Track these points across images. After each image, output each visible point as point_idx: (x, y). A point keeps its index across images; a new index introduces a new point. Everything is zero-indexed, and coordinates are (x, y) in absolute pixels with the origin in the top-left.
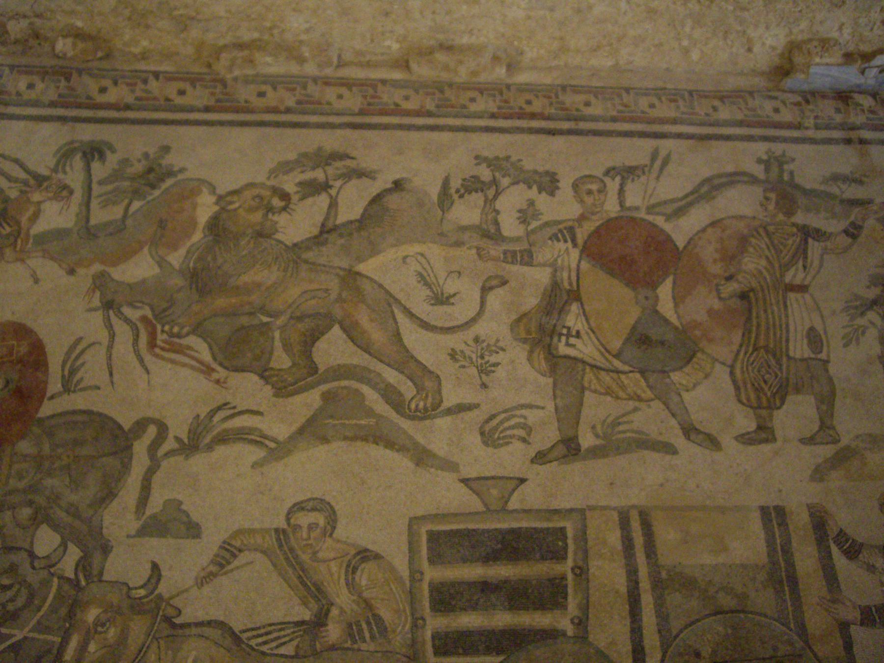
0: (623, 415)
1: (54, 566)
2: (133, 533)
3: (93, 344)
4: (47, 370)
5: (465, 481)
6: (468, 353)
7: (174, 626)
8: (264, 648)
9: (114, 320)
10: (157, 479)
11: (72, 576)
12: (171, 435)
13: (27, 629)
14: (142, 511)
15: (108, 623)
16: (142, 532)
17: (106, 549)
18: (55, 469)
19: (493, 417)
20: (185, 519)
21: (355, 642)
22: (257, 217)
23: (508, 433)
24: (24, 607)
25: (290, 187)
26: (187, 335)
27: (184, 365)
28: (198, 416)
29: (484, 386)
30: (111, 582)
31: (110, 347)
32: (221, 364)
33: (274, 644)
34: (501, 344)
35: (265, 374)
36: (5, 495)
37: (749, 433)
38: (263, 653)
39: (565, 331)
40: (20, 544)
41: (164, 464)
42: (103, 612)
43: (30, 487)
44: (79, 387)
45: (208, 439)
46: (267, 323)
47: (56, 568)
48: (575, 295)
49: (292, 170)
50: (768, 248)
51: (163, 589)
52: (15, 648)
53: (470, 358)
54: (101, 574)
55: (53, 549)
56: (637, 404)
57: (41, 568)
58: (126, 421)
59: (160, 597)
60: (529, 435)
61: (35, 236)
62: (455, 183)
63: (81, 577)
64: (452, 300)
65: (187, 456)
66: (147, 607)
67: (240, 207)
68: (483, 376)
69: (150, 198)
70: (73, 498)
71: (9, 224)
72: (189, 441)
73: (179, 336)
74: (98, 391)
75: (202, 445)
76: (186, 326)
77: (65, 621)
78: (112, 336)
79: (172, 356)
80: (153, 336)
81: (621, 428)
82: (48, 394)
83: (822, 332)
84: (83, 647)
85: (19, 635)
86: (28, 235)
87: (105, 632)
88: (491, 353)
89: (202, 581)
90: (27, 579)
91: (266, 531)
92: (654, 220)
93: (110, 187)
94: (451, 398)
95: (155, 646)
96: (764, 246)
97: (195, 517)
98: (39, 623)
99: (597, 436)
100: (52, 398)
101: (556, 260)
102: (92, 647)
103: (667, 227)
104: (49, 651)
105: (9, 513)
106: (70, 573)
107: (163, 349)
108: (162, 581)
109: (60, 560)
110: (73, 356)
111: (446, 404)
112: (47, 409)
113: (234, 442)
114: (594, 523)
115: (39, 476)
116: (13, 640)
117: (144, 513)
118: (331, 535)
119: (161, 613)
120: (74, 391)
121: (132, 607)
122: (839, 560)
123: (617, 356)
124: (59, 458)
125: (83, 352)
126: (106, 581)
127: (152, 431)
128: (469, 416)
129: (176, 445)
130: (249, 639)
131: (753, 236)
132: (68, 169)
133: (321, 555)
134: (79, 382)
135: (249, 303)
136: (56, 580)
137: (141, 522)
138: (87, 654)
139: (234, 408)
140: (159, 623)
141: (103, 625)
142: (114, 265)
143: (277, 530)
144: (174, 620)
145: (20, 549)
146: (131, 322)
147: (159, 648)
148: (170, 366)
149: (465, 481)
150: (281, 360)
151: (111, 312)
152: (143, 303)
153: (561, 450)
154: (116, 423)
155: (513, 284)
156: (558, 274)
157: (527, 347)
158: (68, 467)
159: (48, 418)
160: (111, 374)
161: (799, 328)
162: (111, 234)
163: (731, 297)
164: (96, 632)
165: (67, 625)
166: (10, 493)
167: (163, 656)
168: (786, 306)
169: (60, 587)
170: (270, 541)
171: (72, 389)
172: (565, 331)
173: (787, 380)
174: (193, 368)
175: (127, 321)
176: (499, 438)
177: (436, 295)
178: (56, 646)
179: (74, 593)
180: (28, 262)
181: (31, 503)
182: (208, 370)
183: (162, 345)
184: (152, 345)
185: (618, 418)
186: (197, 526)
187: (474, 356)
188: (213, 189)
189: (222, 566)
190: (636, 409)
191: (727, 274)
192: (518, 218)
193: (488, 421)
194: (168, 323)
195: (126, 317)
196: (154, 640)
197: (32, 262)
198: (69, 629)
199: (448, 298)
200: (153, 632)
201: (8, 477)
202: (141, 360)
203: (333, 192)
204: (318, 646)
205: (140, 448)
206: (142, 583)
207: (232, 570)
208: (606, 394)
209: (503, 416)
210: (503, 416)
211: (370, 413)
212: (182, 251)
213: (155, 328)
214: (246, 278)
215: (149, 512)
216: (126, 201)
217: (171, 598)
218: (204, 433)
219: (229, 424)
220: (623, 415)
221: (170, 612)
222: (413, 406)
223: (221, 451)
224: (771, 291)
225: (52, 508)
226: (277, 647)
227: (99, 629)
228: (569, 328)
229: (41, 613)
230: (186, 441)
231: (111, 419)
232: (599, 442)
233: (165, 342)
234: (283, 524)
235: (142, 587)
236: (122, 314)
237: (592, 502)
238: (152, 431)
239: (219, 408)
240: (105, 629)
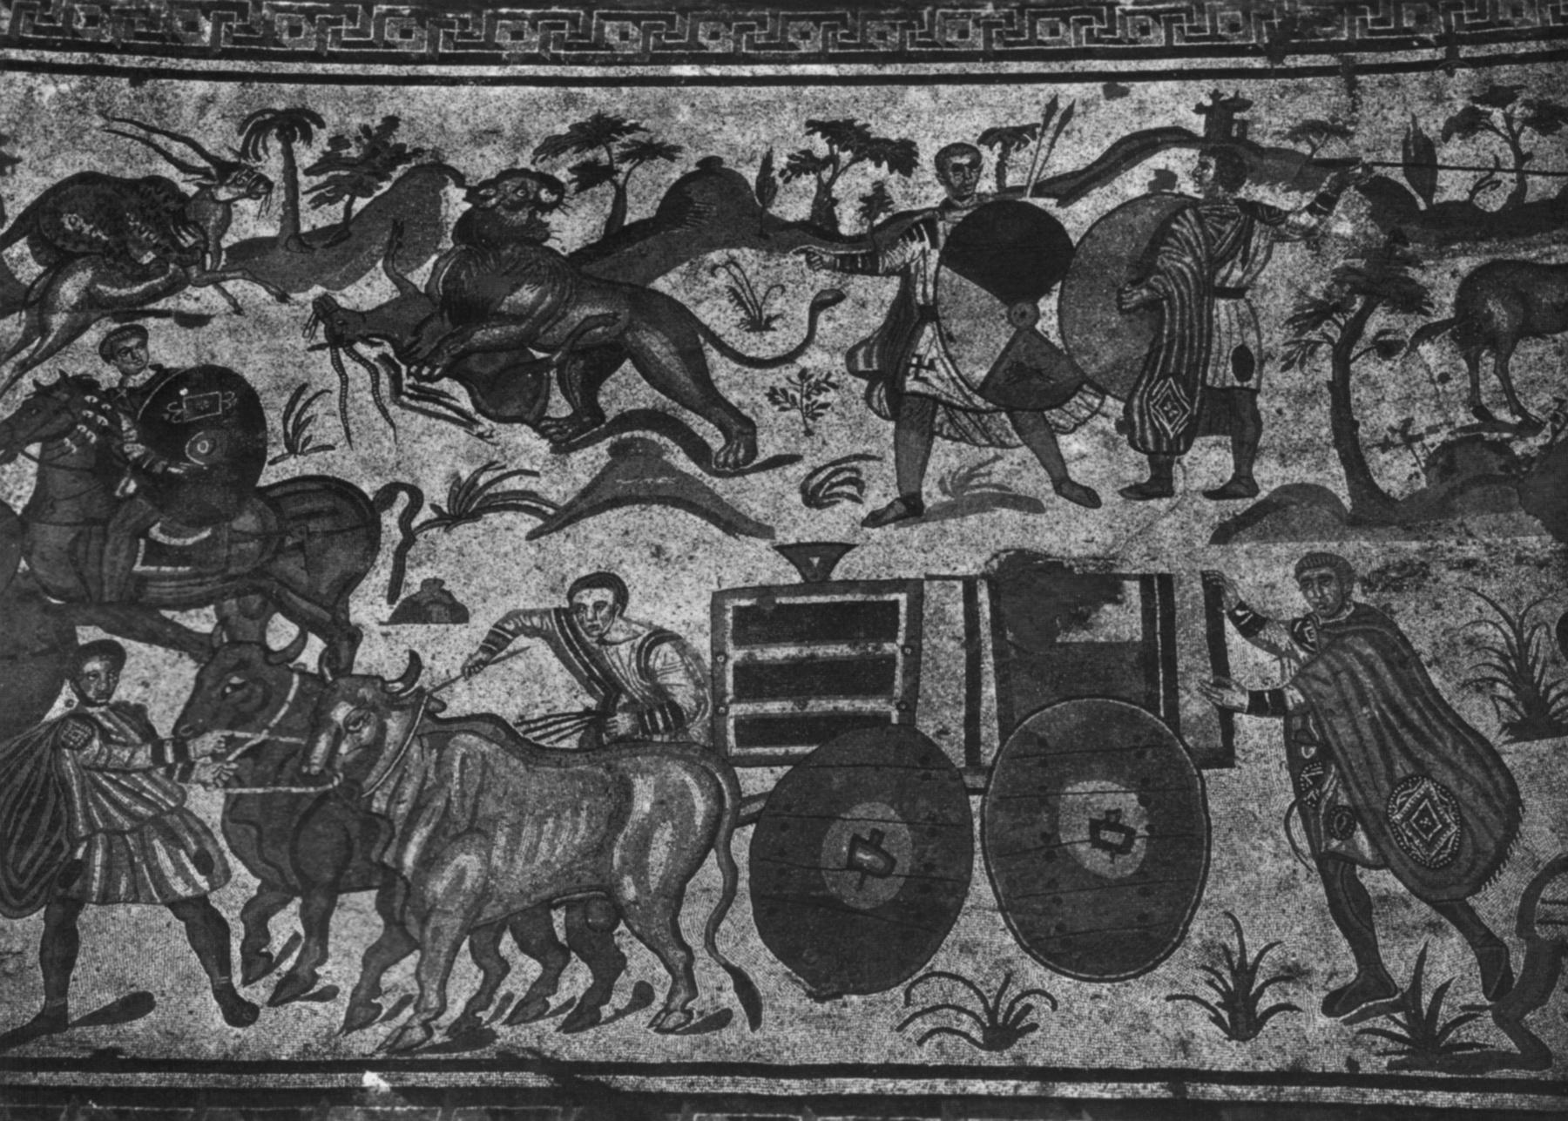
0: (980, 465)
2: (386, 619)
3: (323, 392)
5: (783, 549)
6: (791, 392)
8: (544, 742)
12: (426, 505)
16: (396, 619)
19: (817, 471)
20: (449, 602)
21: (645, 731)
22: (522, 216)
23: (836, 490)
25: (562, 175)
26: (439, 378)
27: (438, 416)
29: (809, 433)
33: (553, 738)
34: (833, 379)
35: (539, 425)
38: (543, 748)
39: (914, 361)
41: (420, 537)
43: (256, 569)
48: (930, 313)
49: (564, 149)
51: (424, 681)
52: (255, 752)
53: (793, 397)
56: (999, 451)
58: (369, 487)
60: (860, 491)
61: (229, 250)
63: (326, 671)
64: (774, 325)
67: (498, 203)
68: (809, 421)
69: (378, 193)
78: (345, 381)
80: (396, 379)
81: (975, 482)
82: (269, 458)
86: (219, 249)
88: (820, 391)
91: (547, 612)
93: (323, 178)
94: (768, 447)
95: (415, 747)
99: (945, 492)
100: (273, 462)
102: (344, 749)
103: (1059, 213)
106: (312, 665)
107: (411, 397)
111: (761, 458)
114: (933, 591)
116: (249, 744)
118: (621, 615)
120: (302, 453)
122: (1234, 637)
125: (309, 403)
127: (403, 497)
128: (790, 471)
130: (525, 732)
132: (261, 152)
133: (607, 637)
134: (309, 439)
139: (504, 467)
142: (340, 288)
143: (557, 610)
149: (783, 549)
150: (560, 406)
153: (901, 508)
157: (865, 383)
158: (300, 547)
169: (302, 683)
170: (550, 624)
172: (914, 361)
176: (824, 496)
177: (753, 318)
181: (257, 590)
182: (467, 421)
184: (397, 390)
185: (972, 469)
187: (798, 396)
188: (460, 180)
189: (493, 653)
190: (997, 458)
192: (862, 209)
193: (810, 477)
197: (229, 286)
199: (770, 319)
202: (384, 412)
203: (621, 178)
204: (605, 738)
205: (390, 521)
207: (503, 658)
208: (962, 439)
209: (831, 469)
210: (831, 469)
211: (669, 470)
213: (398, 369)
216: (347, 198)
220: (980, 465)
222: (721, 460)
226: (558, 740)
228: (919, 357)
230: (445, 509)
232: (946, 499)
233: (410, 386)
234: (566, 605)
235: (399, 680)
237: (934, 571)
238: (403, 497)
239: (485, 469)
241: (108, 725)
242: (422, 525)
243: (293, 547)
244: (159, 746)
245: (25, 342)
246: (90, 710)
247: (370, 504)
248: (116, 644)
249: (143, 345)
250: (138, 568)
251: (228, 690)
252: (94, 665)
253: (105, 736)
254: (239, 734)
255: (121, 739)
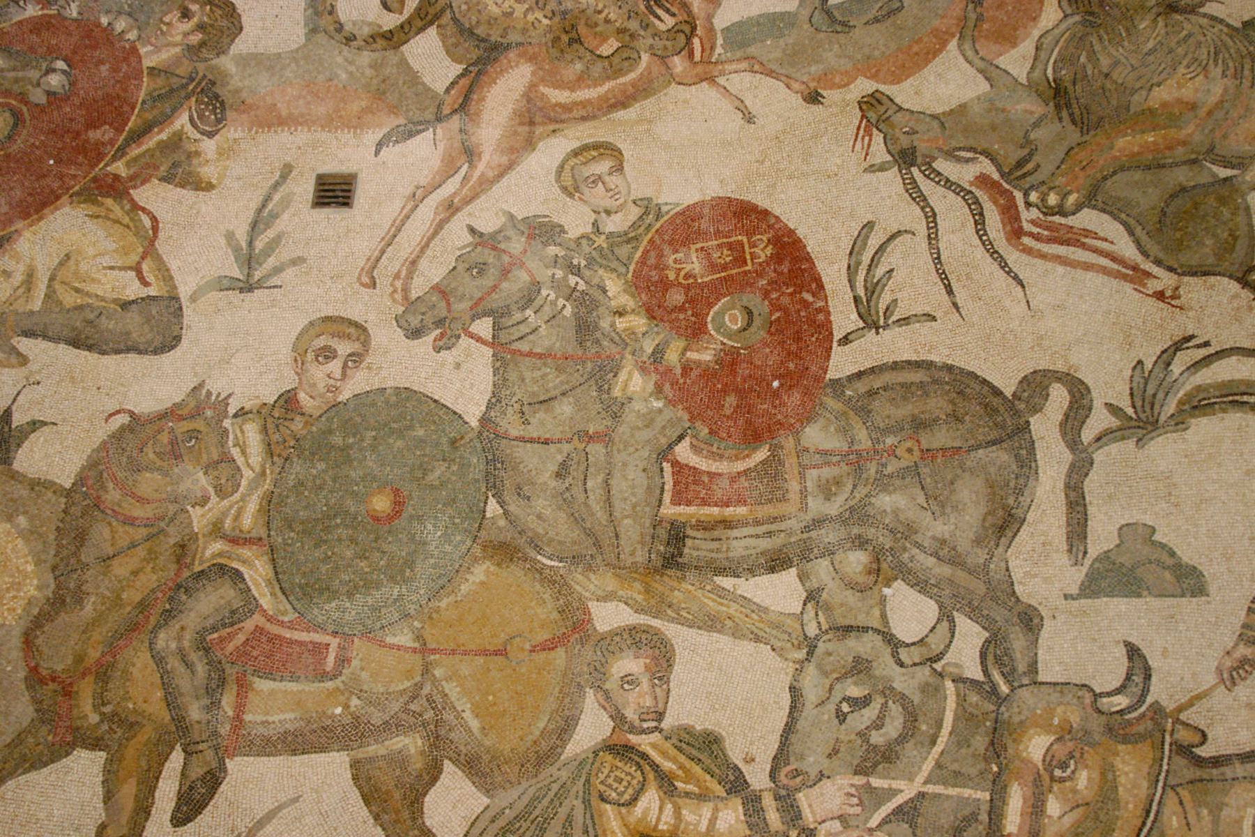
1: (939, 657)
2: (1074, 590)
3: (899, 233)
4: (821, 287)
7: (1199, 762)
9: (926, 186)
10: (1093, 484)
11: (979, 676)
12: (1098, 404)
13: (920, 779)
14: (1082, 548)
15: (1072, 762)
16: (1091, 588)
17: (1030, 621)
18: (890, 476)
20: (1170, 561)
24: (902, 739)
26: (1078, 208)
27: (1088, 267)
28: (1140, 362)
30: (1055, 684)
31: (933, 237)
32: (1158, 262)
36: (807, 529)
40: (862, 620)
41: (1098, 457)
42: (1059, 739)
44: (894, 318)
45: (1171, 407)
46: (1225, 180)
47: (943, 662)
51: (1158, 692)
52: (907, 813)
54: (1033, 668)
55: (929, 628)
57: (915, 664)
59: (1157, 708)
61: (726, 30)
65: (1139, 440)
66: (1140, 728)
70: (940, 528)
71: (668, 11)
72: (1136, 412)
73: (1061, 211)
74: (934, 323)
75: (1163, 418)
76: (1069, 193)
77: (986, 760)
78: (932, 218)
79: (1061, 250)
80: (1010, 213)
82: (837, 335)
84: (1036, 808)
85: (907, 791)
86: (711, 30)
87: (1070, 778)
89: (1232, 678)
90: (895, 685)
95: (1171, 800)
97: (1187, 555)
98: (939, 765)
100: (845, 340)
102: (1053, 807)
104: (972, 818)
105: (824, 563)
107: (1037, 237)
108: (1154, 679)
109: (948, 646)
110: (866, 258)
112: (842, 363)
113: (1224, 411)
115: (861, 492)
116: (899, 800)
117: (1085, 553)
119: (1168, 739)
120: (886, 326)
121: (1110, 729)
124: (892, 452)
125: (881, 249)
126: (1043, 683)
127: (1059, 396)
129: (1114, 422)
135: (1184, 143)
136: (949, 684)
137: (1084, 570)
138: (1046, 821)
139: (1206, 344)
140: (1170, 758)
141: (1063, 766)
142: (897, 80)
144: (1197, 751)
145: (865, 629)
146: (963, 189)
147: (1181, 803)
148: (1060, 269)
151: (915, 170)
152: (971, 149)
154: (985, 382)
158: (914, 470)
159: (850, 378)
160: (950, 291)
162: (876, 20)
164: (1052, 779)
165: (995, 769)
166: (818, 523)
167: (1192, 819)
169: (961, 700)
171: (882, 322)
174: (1105, 271)
175: (949, 184)
178: (985, 807)
179: (992, 707)
180: (721, 81)
181: (861, 543)
182: (1137, 276)
183: (1035, 230)
186: (1194, 572)
194: (1032, 187)
195: (948, 180)
196: (1168, 790)
198: (999, 773)
200: (1163, 774)
201: (804, 493)
202: (1004, 265)
206: (1117, 683)
212: (1027, 47)
214: (1162, 95)
215: (1093, 552)
217: (1180, 709)
218: (1160, 395)
219: (1205, 376)
221: (1184, 736)
223: (1202, 427)
225: (905, 549)
227: (1058, 773)
229: (938, 748)
230: (1130, 411)
231: (973, 375)
233: (1033, 222)
235: (1118, 691)
236: (939, 174)
238: (1059, 396)
240: (1069, 771)
241: (667, 765)
242: (1098, 439)
243: (902, 474)
244: (753, 803)
245: (449, 170)
246: (634, 739)
247: (1010, 404)
248: (657, 632)
249: (619, 168)
250: (669, 510)
251: (845, 708)
252: (629, 664)
253: (666, 783)
254: (876, 782)
255: (690, 788)
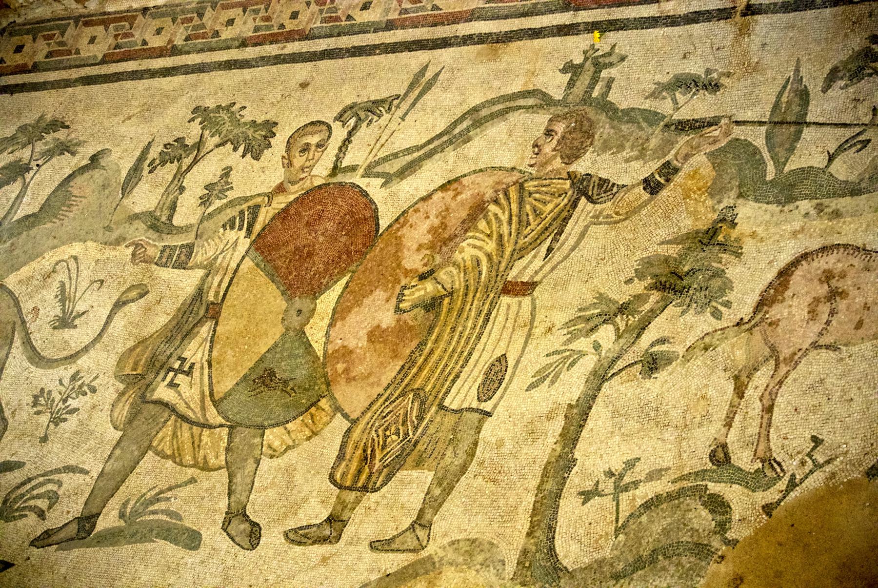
37: (309, 526)
50: (510, 222)
62: (154, 153)
83: (511, 363)
92: (368, 185)
96: (504, 218)
101: (216, 258)
123: (215, 403)
131: (496, 202)
155: (150, 297)
156: (210, 278)
161: (485, 356)
163: (415, 306)
168: (487, 320)
173: (417, 442)
191: (426, 269)
224: (478, 295)
